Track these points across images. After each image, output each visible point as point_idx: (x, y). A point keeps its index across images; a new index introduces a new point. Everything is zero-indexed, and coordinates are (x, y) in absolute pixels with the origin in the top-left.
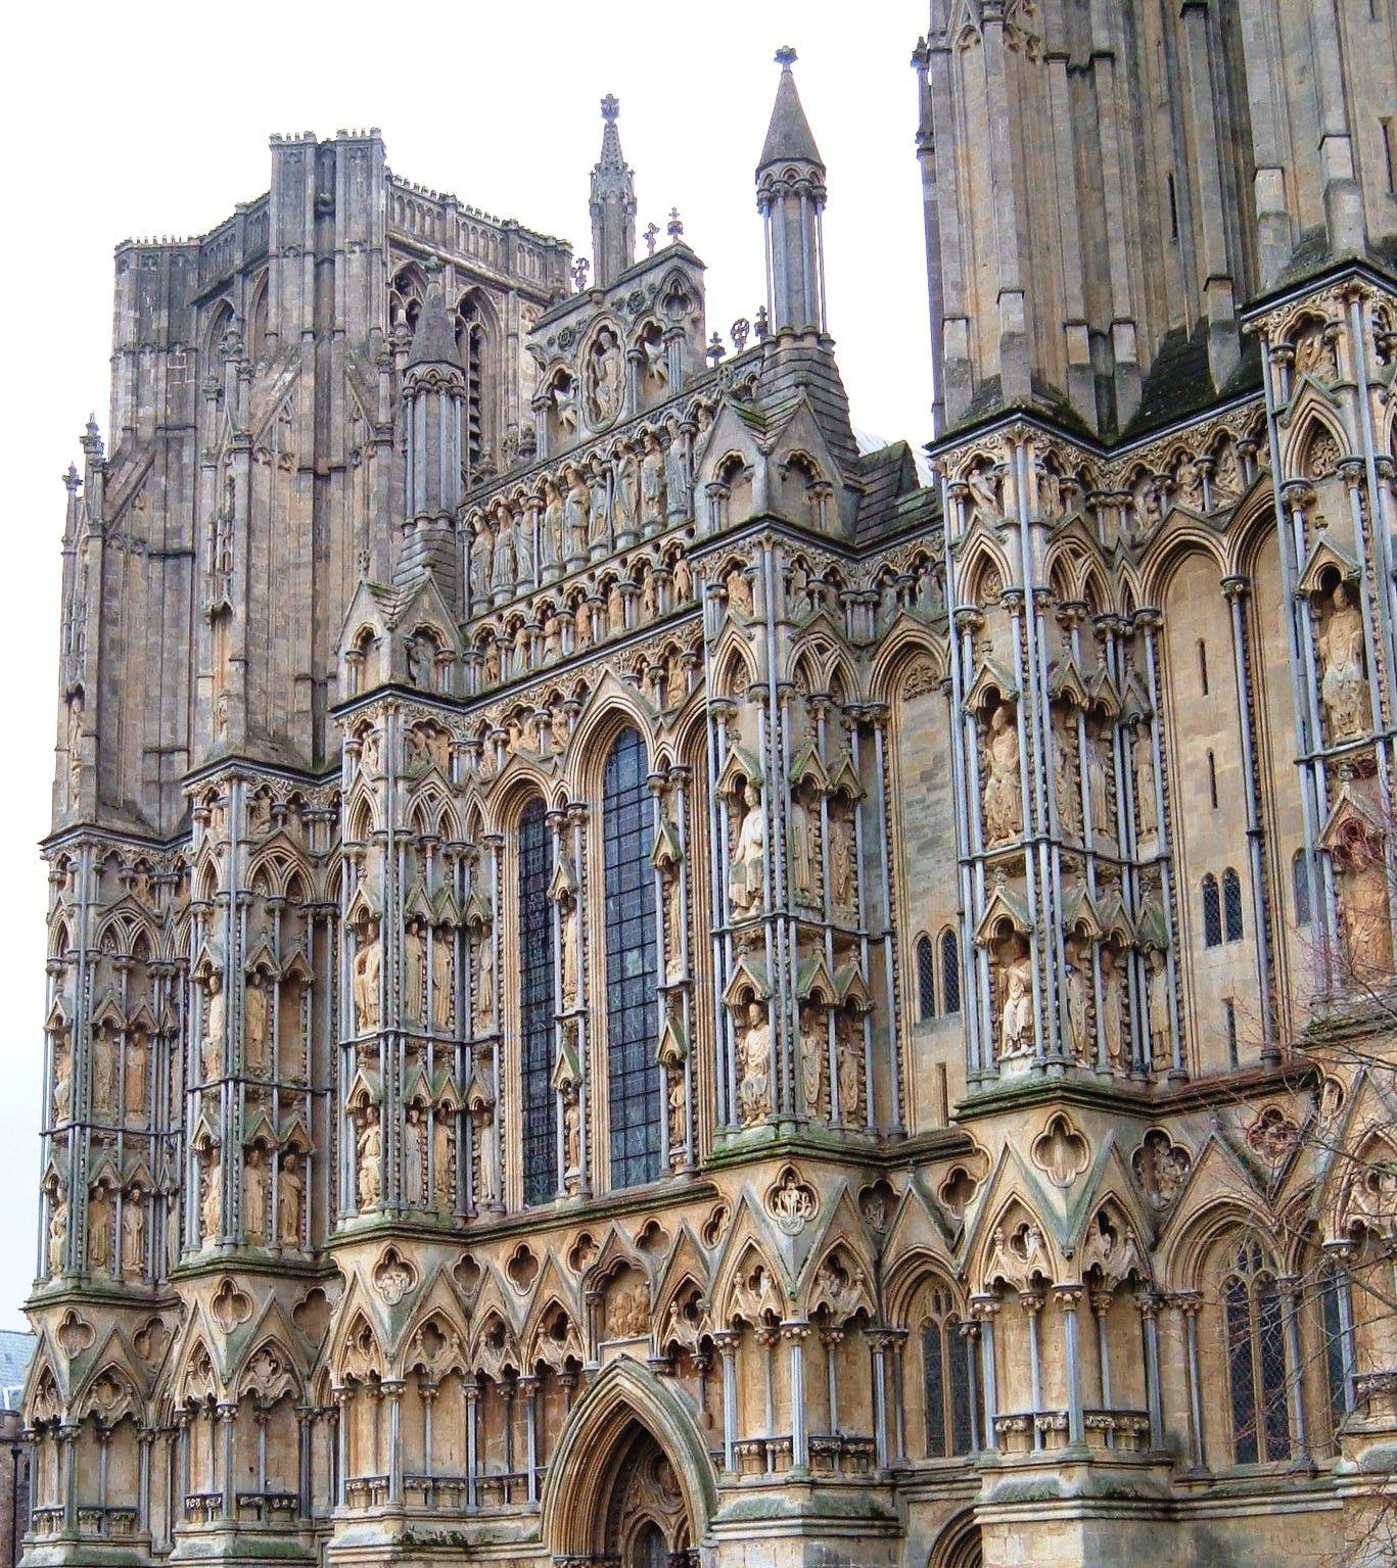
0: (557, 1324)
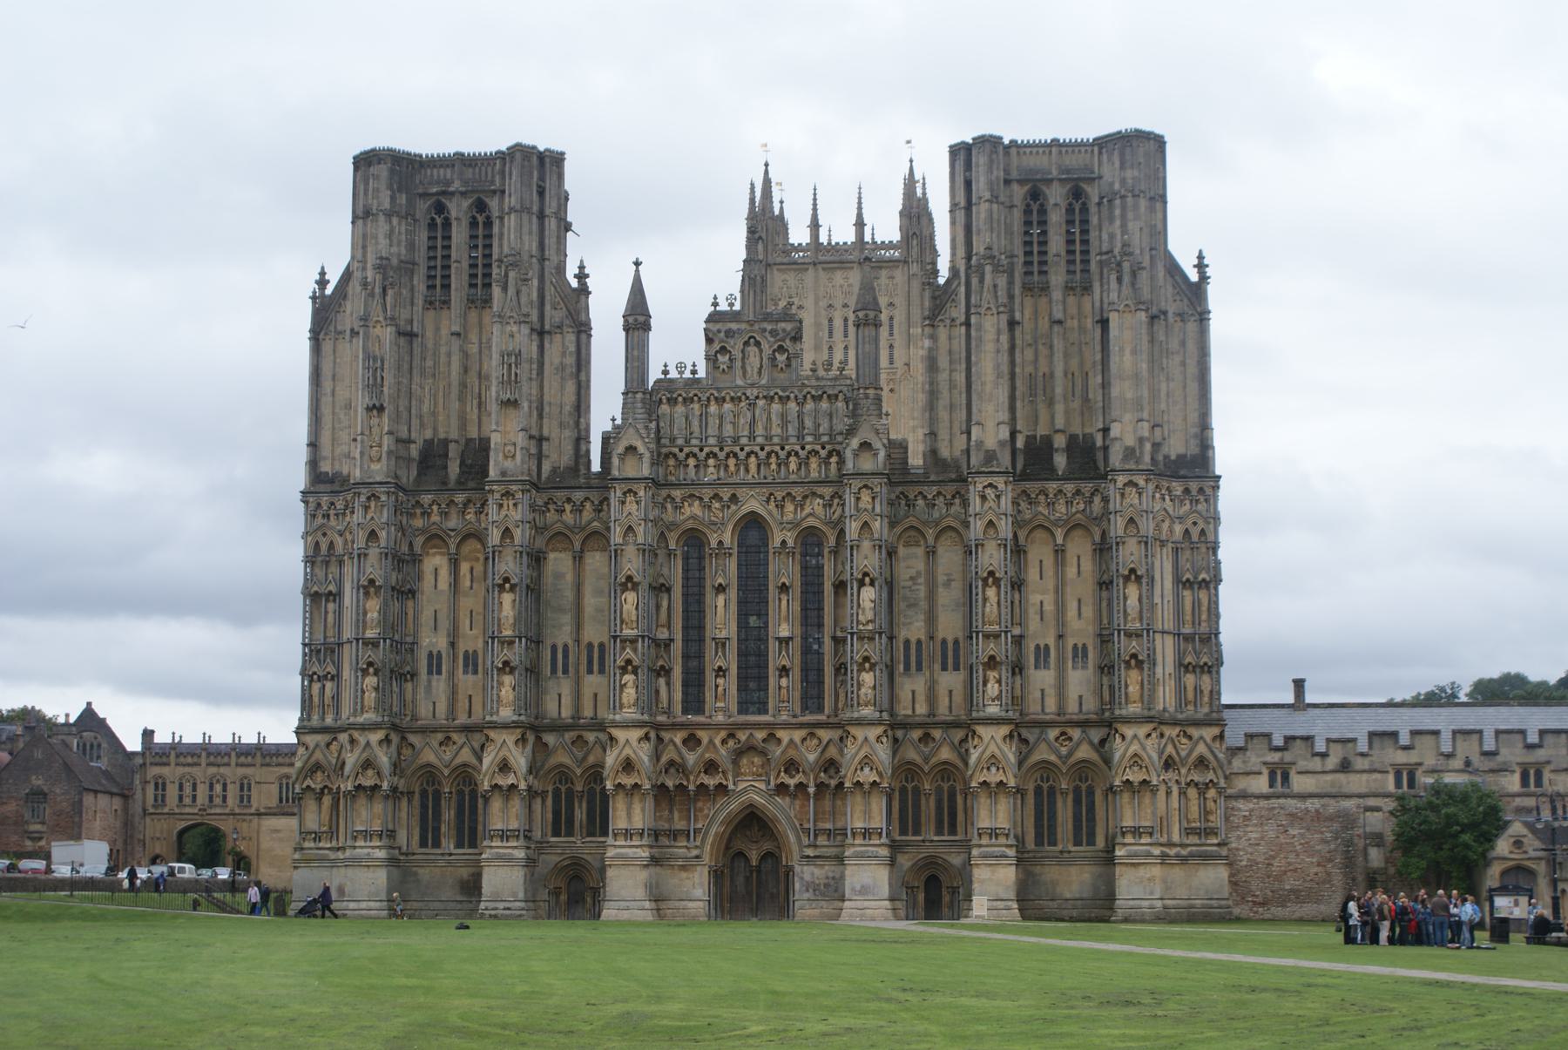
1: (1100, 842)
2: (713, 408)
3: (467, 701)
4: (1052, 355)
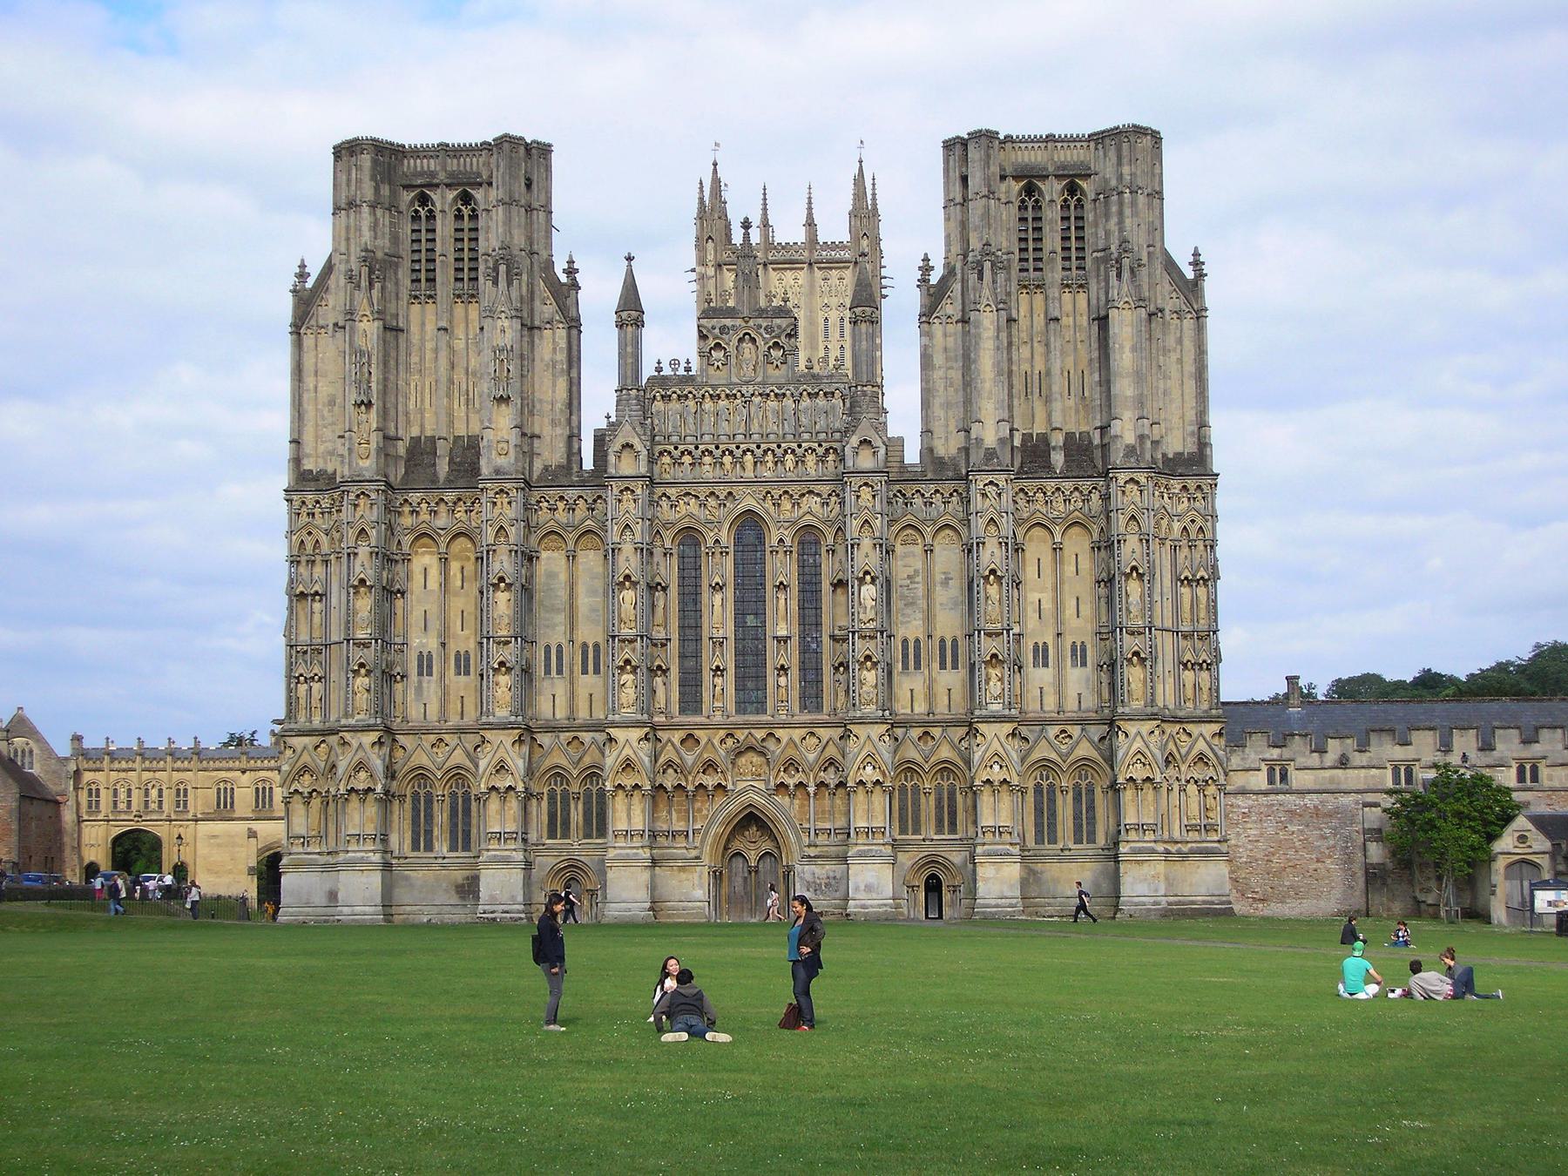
0: (710, 766)
1: (1101, 840)
2: (708, 405)
4: (1048, 352)
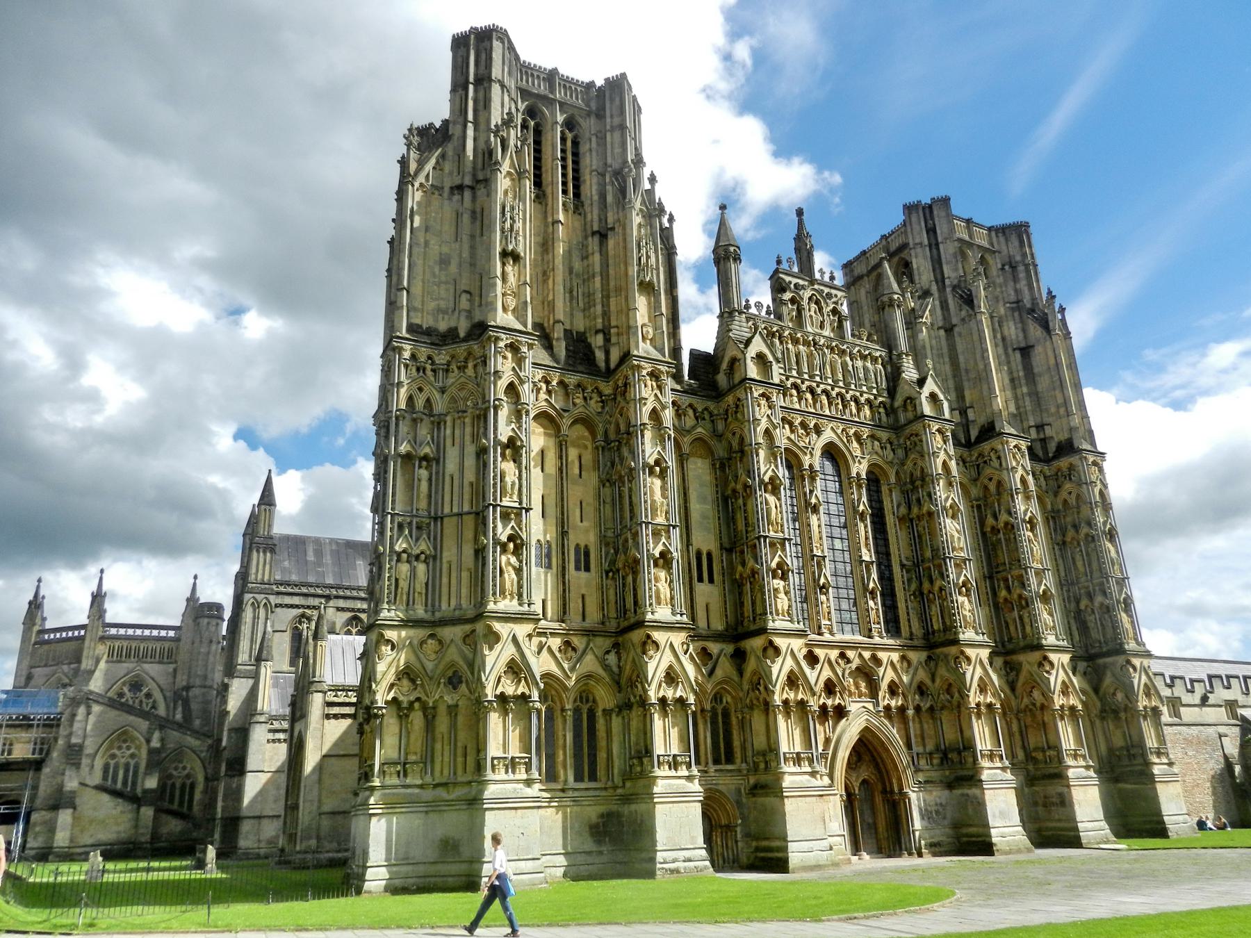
3: (580, 601)
